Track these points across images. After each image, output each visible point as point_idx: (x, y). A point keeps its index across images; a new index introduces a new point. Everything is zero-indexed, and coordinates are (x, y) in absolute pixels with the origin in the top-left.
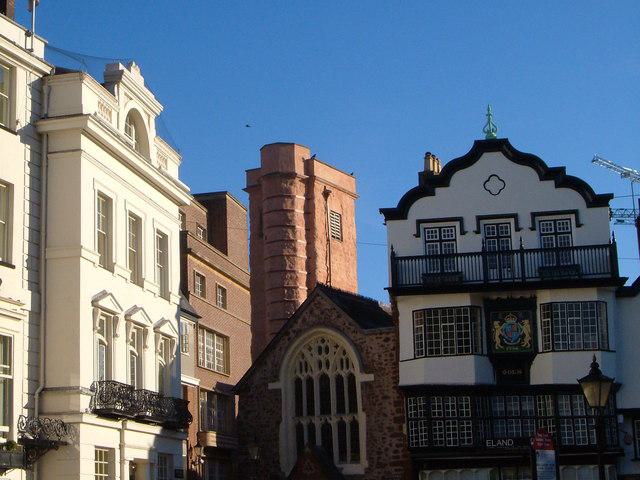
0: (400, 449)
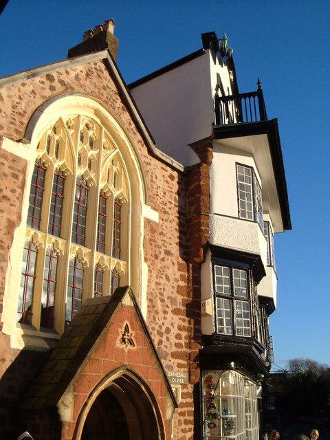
0: (184, 334)
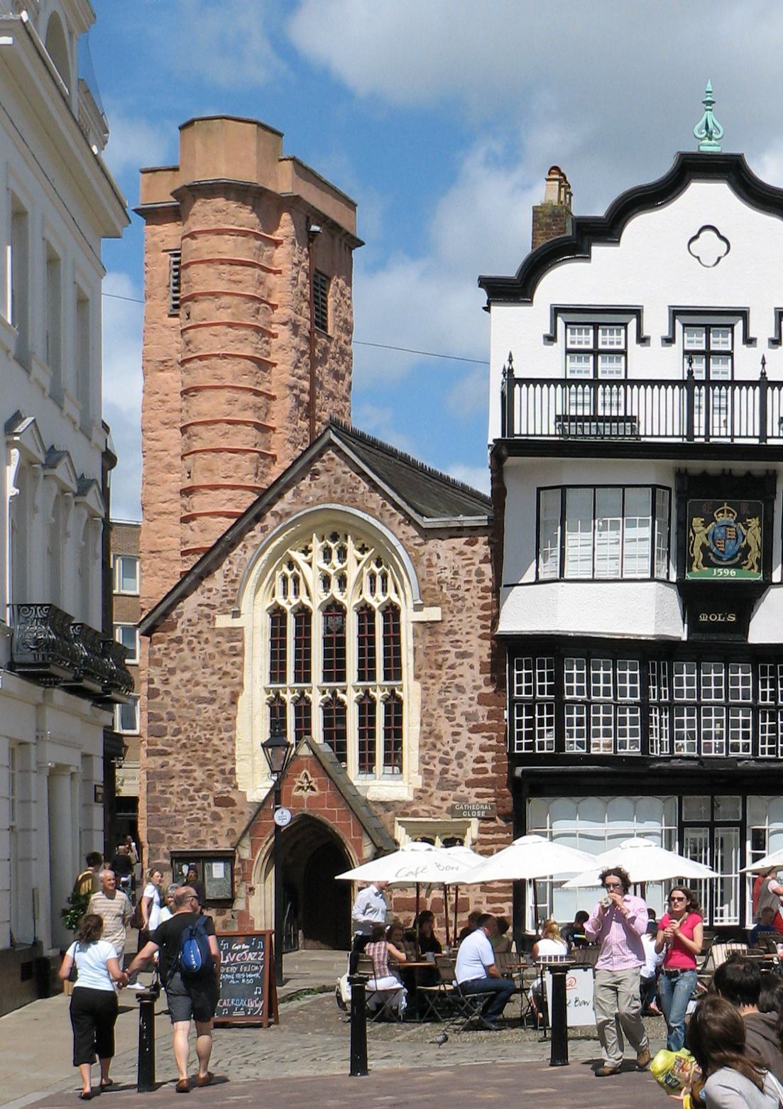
0: (489, 755)
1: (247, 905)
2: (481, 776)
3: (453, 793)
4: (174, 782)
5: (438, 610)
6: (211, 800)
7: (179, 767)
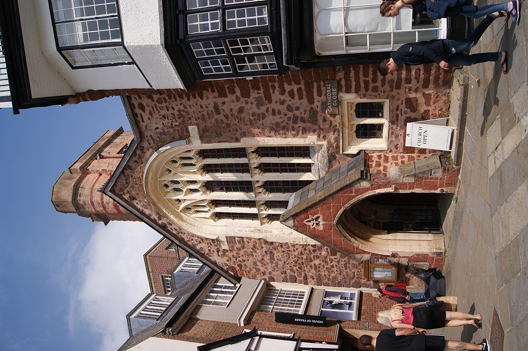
0: (287, 88)
1: (405, 257)
2: (304, 93)
3: (320, 114)
4: (323, 274)
5: (190, 128)
6: (332, 257)
7: (313, 271)
